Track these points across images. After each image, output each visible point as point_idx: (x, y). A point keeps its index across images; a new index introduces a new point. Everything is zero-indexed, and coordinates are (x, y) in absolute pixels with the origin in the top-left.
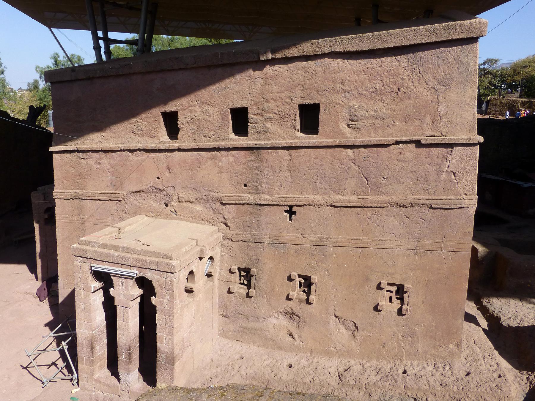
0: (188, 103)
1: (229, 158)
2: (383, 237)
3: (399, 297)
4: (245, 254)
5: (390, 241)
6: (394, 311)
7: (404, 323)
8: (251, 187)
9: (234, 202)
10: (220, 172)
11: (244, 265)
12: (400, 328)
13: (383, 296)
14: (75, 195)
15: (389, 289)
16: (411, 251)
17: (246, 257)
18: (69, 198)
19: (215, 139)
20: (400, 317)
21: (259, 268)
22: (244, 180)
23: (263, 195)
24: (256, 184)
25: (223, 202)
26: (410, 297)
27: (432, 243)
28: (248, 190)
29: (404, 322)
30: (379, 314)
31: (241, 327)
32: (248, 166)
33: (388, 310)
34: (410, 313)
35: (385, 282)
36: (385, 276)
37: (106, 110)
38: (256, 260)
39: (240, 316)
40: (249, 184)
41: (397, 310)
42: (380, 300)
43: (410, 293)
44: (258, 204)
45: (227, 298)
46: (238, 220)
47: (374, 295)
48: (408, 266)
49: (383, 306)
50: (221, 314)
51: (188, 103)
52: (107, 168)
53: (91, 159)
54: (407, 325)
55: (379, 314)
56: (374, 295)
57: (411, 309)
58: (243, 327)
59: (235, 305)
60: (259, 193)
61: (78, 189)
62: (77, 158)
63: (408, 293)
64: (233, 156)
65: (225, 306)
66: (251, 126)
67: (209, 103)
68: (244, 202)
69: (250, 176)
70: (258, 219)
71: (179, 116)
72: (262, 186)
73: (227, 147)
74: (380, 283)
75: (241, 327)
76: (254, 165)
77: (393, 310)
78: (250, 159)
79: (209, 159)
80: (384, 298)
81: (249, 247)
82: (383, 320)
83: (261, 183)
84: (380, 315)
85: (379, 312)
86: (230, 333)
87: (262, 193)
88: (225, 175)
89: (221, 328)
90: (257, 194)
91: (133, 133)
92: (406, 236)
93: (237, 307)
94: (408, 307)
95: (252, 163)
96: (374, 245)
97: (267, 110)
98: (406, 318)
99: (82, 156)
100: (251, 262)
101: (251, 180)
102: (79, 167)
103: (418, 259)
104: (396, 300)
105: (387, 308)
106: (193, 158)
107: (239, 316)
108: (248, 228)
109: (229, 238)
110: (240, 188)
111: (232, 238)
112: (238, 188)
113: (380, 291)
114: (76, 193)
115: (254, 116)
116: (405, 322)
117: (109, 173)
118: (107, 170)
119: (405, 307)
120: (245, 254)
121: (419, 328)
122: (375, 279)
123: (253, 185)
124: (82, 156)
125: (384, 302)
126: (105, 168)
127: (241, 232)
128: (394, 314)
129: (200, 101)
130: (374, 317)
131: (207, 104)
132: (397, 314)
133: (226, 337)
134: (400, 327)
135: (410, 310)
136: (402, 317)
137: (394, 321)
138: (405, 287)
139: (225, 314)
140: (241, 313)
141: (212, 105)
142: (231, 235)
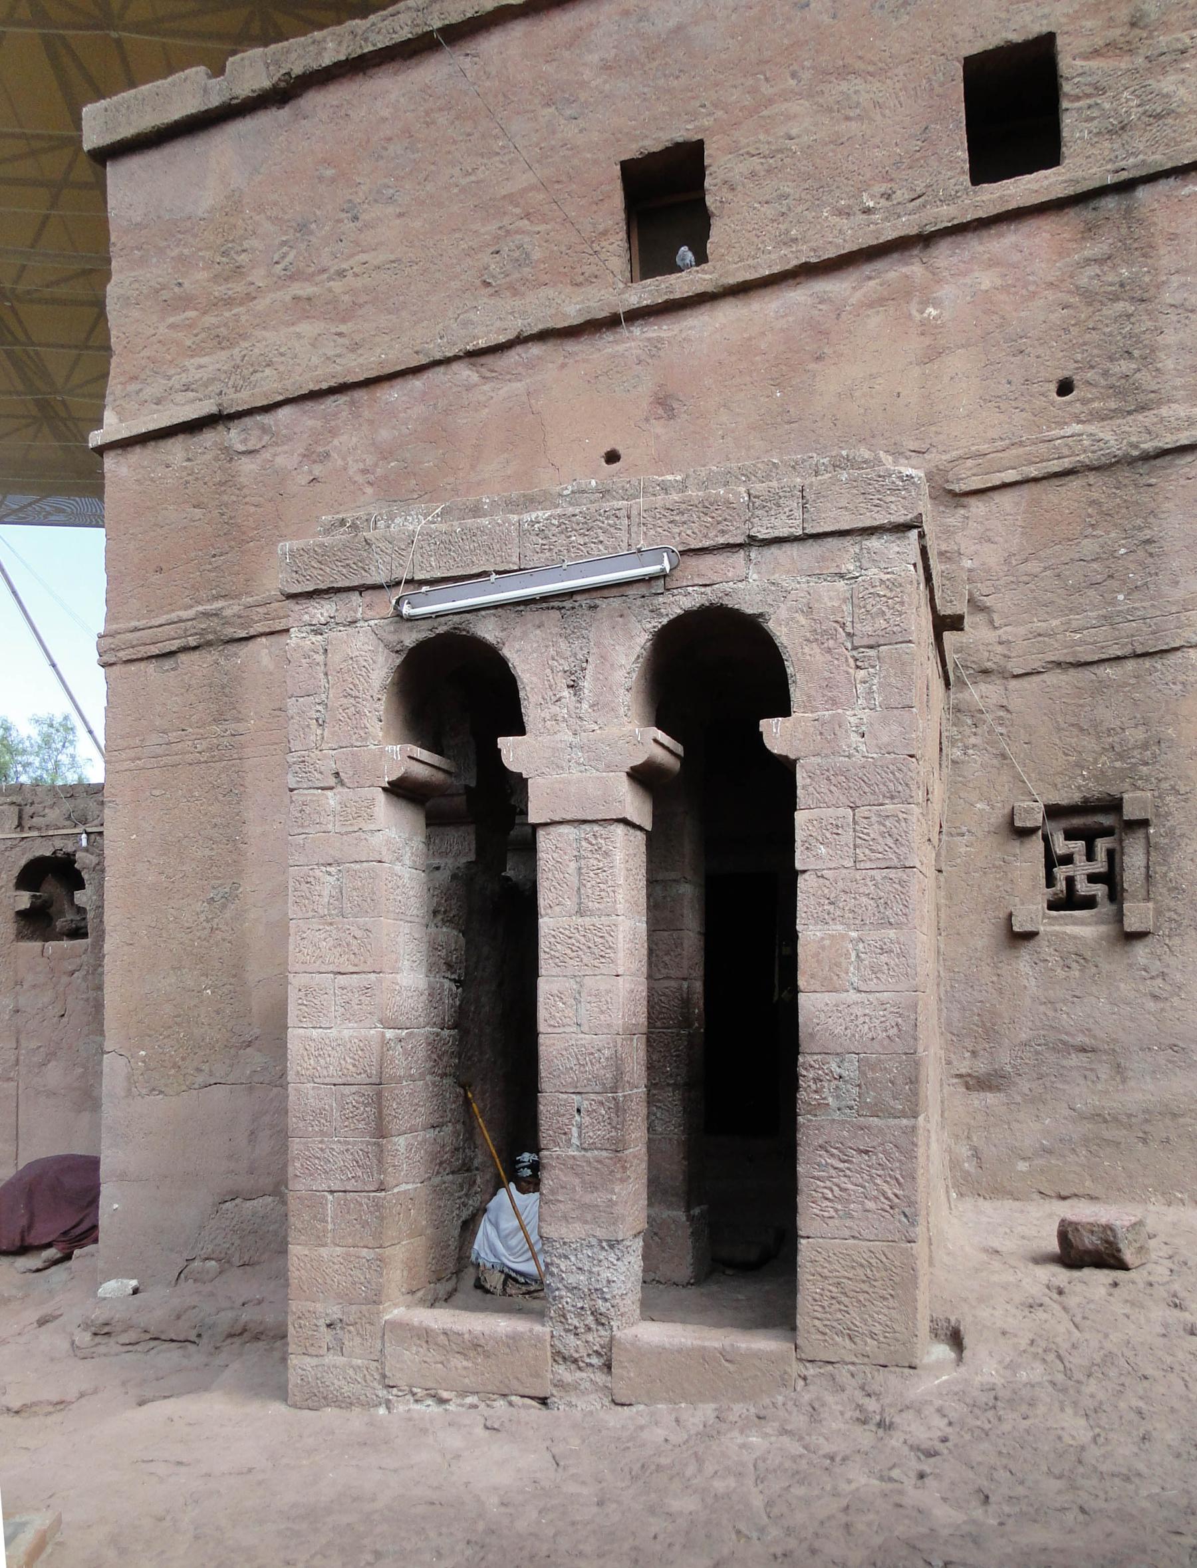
0: (754, 91)
1: (977, 274)
4: (1082, 730)
8: (1095, 386)
9: (1011, 476)
10: (933, 355)
11: (1079, 787)
14: (203, 626)
17: (1089, 743)
18: (174, 645)
19: (899, 209)
21: (1165, 785)
22: (1059, 360)
23: (1164, 411)
24: (1125, 366)
25: (956, 488)
28: (1085, 402)
31: (1082, 1117)
32: (1078, 288)
37: (355, 218)
38: (1145, 746)
39: (1075, 1060)
40: (1090, 375)
44: (1147, 457)
45: (995, 979)
46: (1034, 567)
50: (963, 1071)
51: (754, 91)
52: (361, 466)
53: (283, 443)
58: (1097, 1117)
59: (1042, 1008)
60: (1143, 408)
61: (216, 598)
62: (216, 459)
64: (993, 263)
65: (984, 1025)
66: (1079, 109)
67: (859, 65)
68: (1066, 463)
69: (1088, 336)
70: (1147, 534)
71: (710, 156)
72: (1159, 365)
73: (969, 218)
75: (1082, 1117)
76: (1110, 278)
78: (1087, 253)
79: (871, 305)
81: (1101, 687)
83: (1148, 359)
86: (1022, 1166)
87: (1159, 403)
88: (957, 363)
89: (964, 1151)
90: (1129, 413)
91: (488, 284)
93: (1051, 1014)
95: (1094, 269)
97: (1153, 17)
99: (245, 441)
100: (1118, 764)
101: (1096, 352)
102: (225, 498)
106: (791, 319)
107: (1065, 1063)
108: (1091, 593)
109: (989, 665)
110: (1039, 403)
111: (1002, 662)
112: (1027, 406)
114: (206, 615)
115: (1094, 64)
117: (369, 490)
118: (360, 479)
120: (1082, 730)
123: (1105, 374)
124: (241, 442)
126: (353, 467)
127: (1055, 623)
129: (813, 68)
131: (845, 72)
133: (998, 1191)
139: (981, 1067)
140: (1080, 1039)
141: (871, 68)
142: (1000, 649)
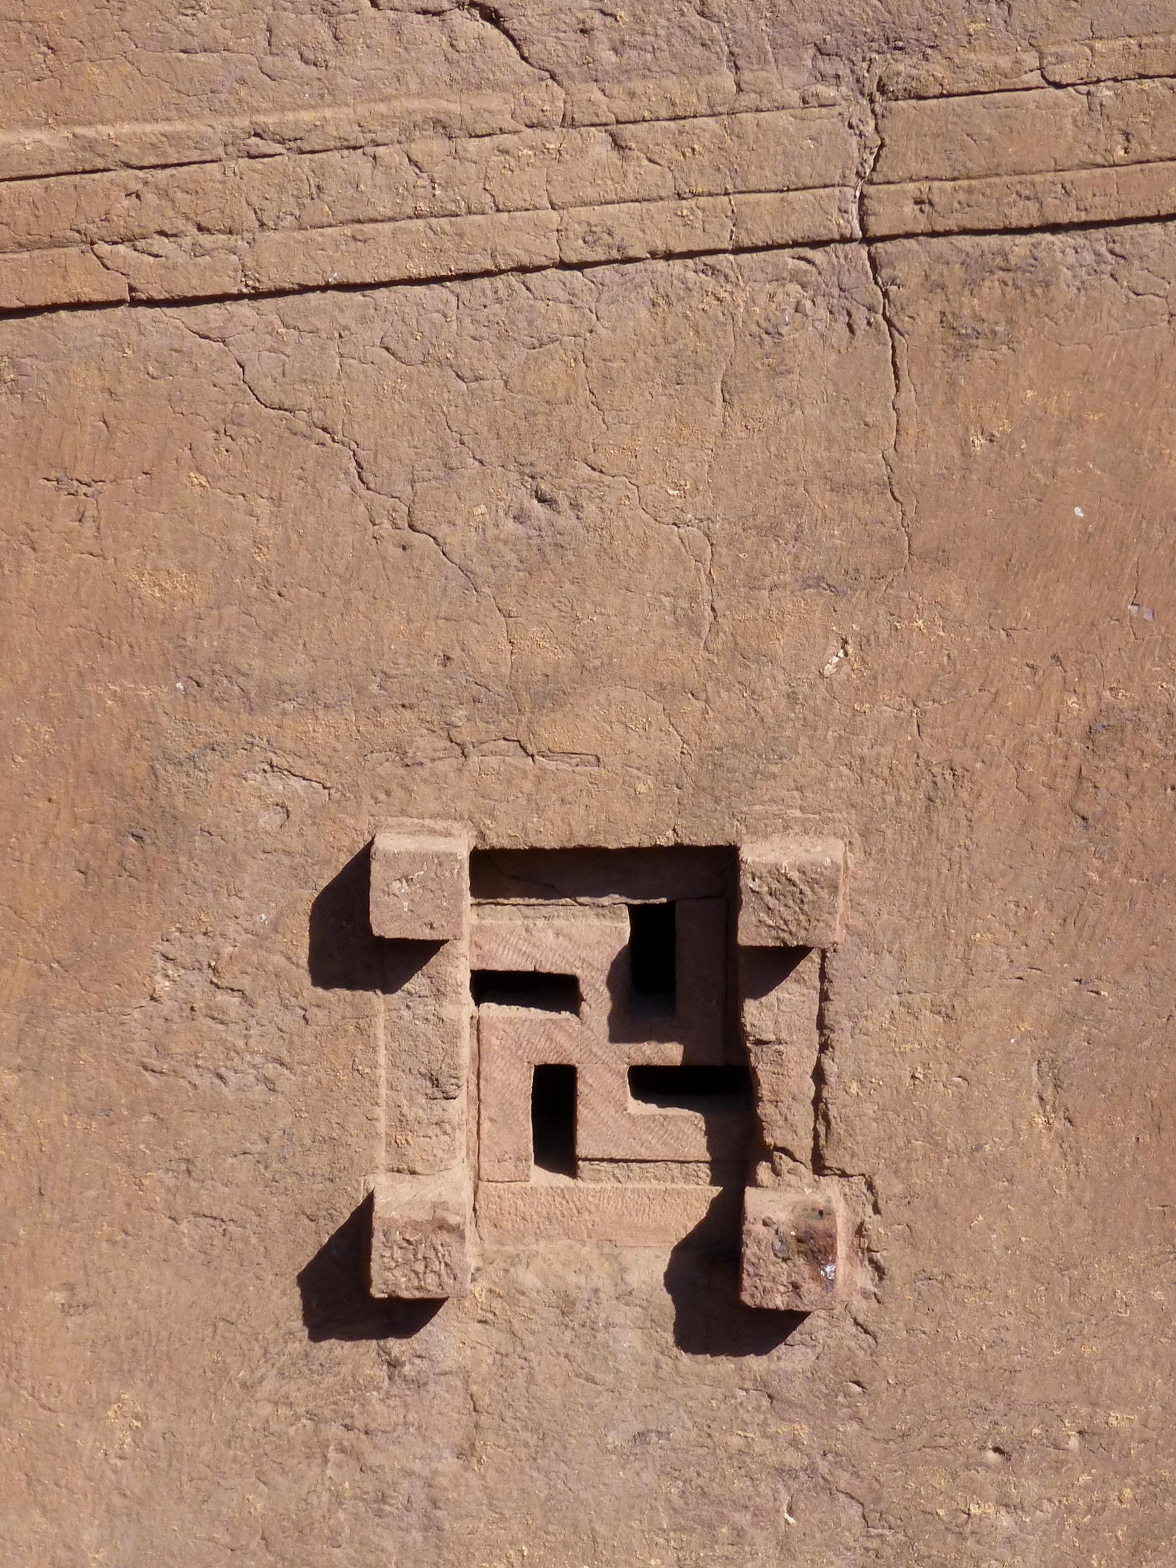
2: (329, 94)
3: (671, 1053)
5: (439, 145)
6: (625, 1296)
7: (792, 1458)
12: (740, 1533)
13: (435, 1082)
15: (506, 960)
16: (795, 277)
20: (726, 1365)
26: (842, 1038)
27: (1105, 93)
29: (795, 1443)
30: (393, 1364)
33: (529, 1279)
34: (864, 1278)
35: (440, 845)
36: (424, 744)
41: (662, 1266)
42: (395, 1145)
43: (835, 967)
47: (287, 1080)
48: (763, 532)
49: (442, 1226)
54: (843, 1479)
55: (393, 1364)
56: (287, 1080)
57: (873, 1223)
63: (815, 956)
74: (360, 867)
77: (601, 1277)
80: (459, 1108)
82: (466, 1452)
84: (419, 1385)
85: (395, 1346)
92: (687, 31)
94: (831, 1192)
96: (197, 251)
98: (813, 1375)
103: (908, 397)
104: (636, 1107)
105: (514, 1260)
113: (377, 1000)
116: (804, 1432)
119: (792, 1197)
121: (1032, 1487)
122: (268, 820)
125: (460, 1172)
128: (630, 1341)
130: (335, 1430)
132: (670, 1338)
134: (743, 1519)
135: (860, 1231)
136: (754, 1363)
137: (641, 1437)
138: (746, 882)
